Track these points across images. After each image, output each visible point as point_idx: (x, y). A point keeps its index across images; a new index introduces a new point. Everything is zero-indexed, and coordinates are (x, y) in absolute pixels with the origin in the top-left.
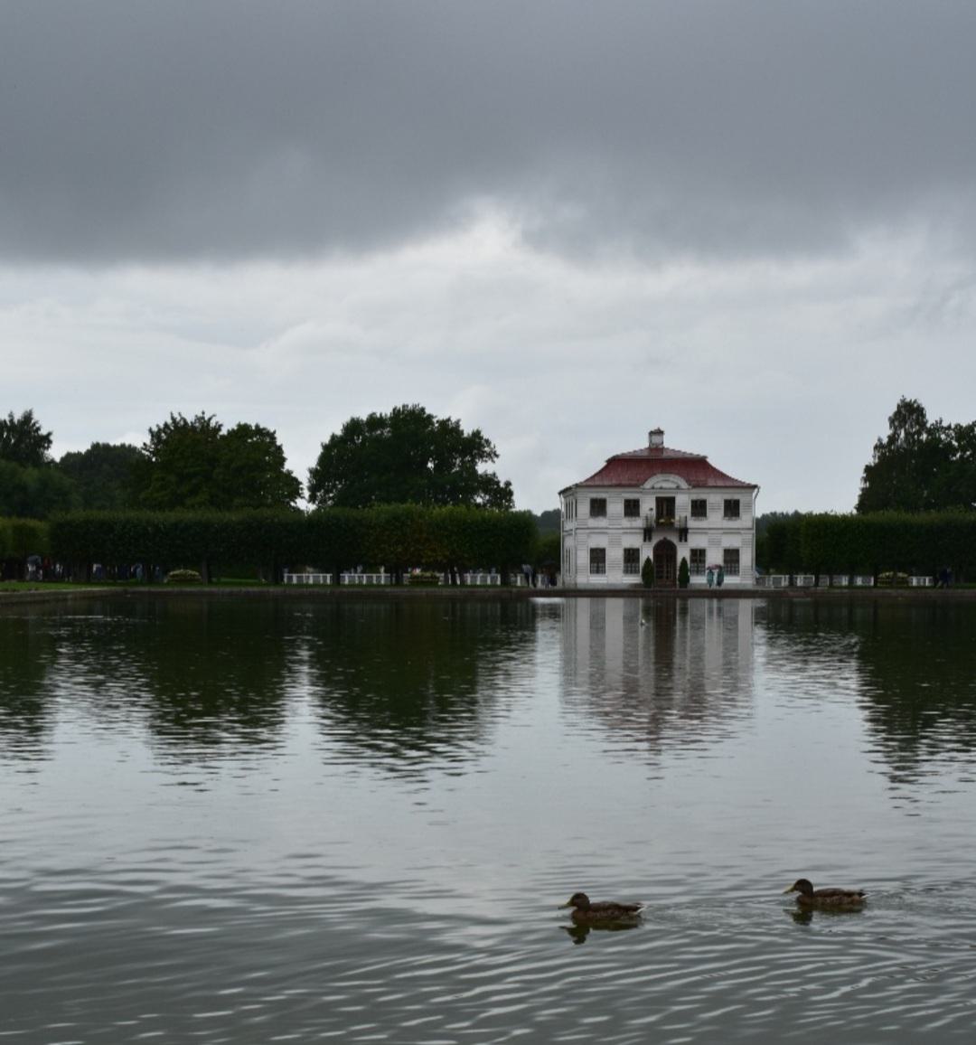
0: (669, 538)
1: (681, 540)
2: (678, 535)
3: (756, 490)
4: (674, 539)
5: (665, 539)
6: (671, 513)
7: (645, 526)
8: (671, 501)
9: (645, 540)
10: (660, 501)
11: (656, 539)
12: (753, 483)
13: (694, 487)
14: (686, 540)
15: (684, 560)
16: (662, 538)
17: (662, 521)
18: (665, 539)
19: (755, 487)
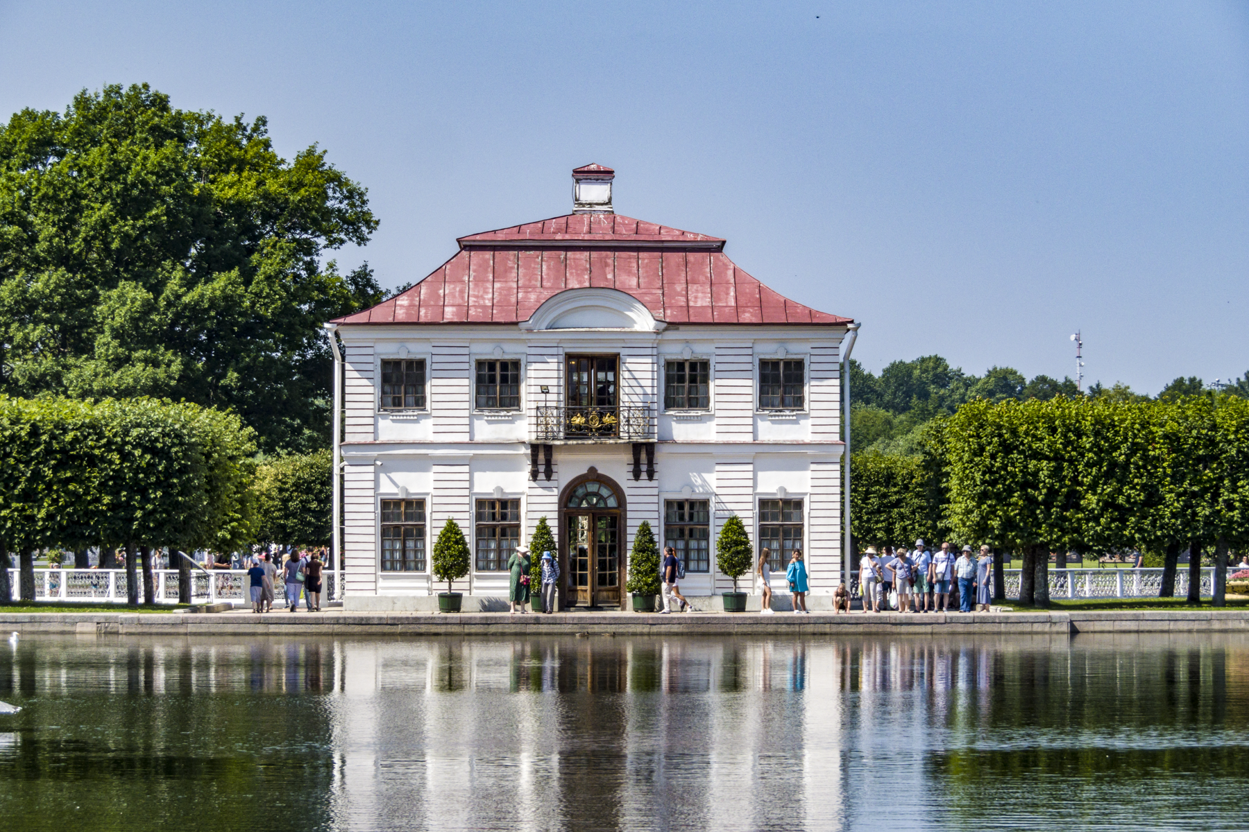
0: (601, 471)
1: (637, 476)
2: (628, 457)
3: (849, 335)
4: (617, 468)
5: (592, 470)
6: (607, 398)
7: (533, 437)
8: (610, 363)
9: (534, 475)
10: (576, 363)
11: (569, 468)
12: (842, 314)
13: (673, 325)
14: (651, 477)
15: (645, 530)
16: (584, 471)
17: (578, 420)
18: (592, 470)
19: (842, 325)
